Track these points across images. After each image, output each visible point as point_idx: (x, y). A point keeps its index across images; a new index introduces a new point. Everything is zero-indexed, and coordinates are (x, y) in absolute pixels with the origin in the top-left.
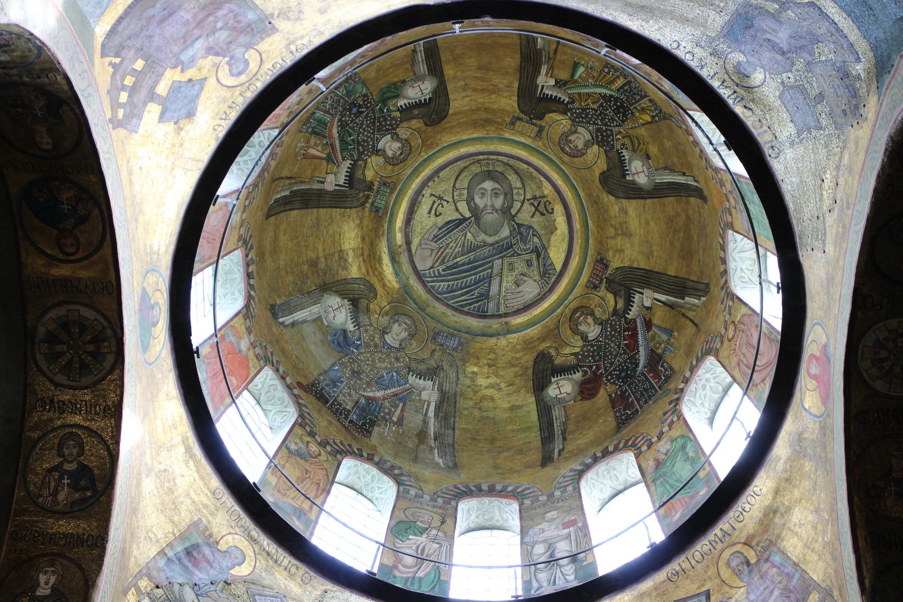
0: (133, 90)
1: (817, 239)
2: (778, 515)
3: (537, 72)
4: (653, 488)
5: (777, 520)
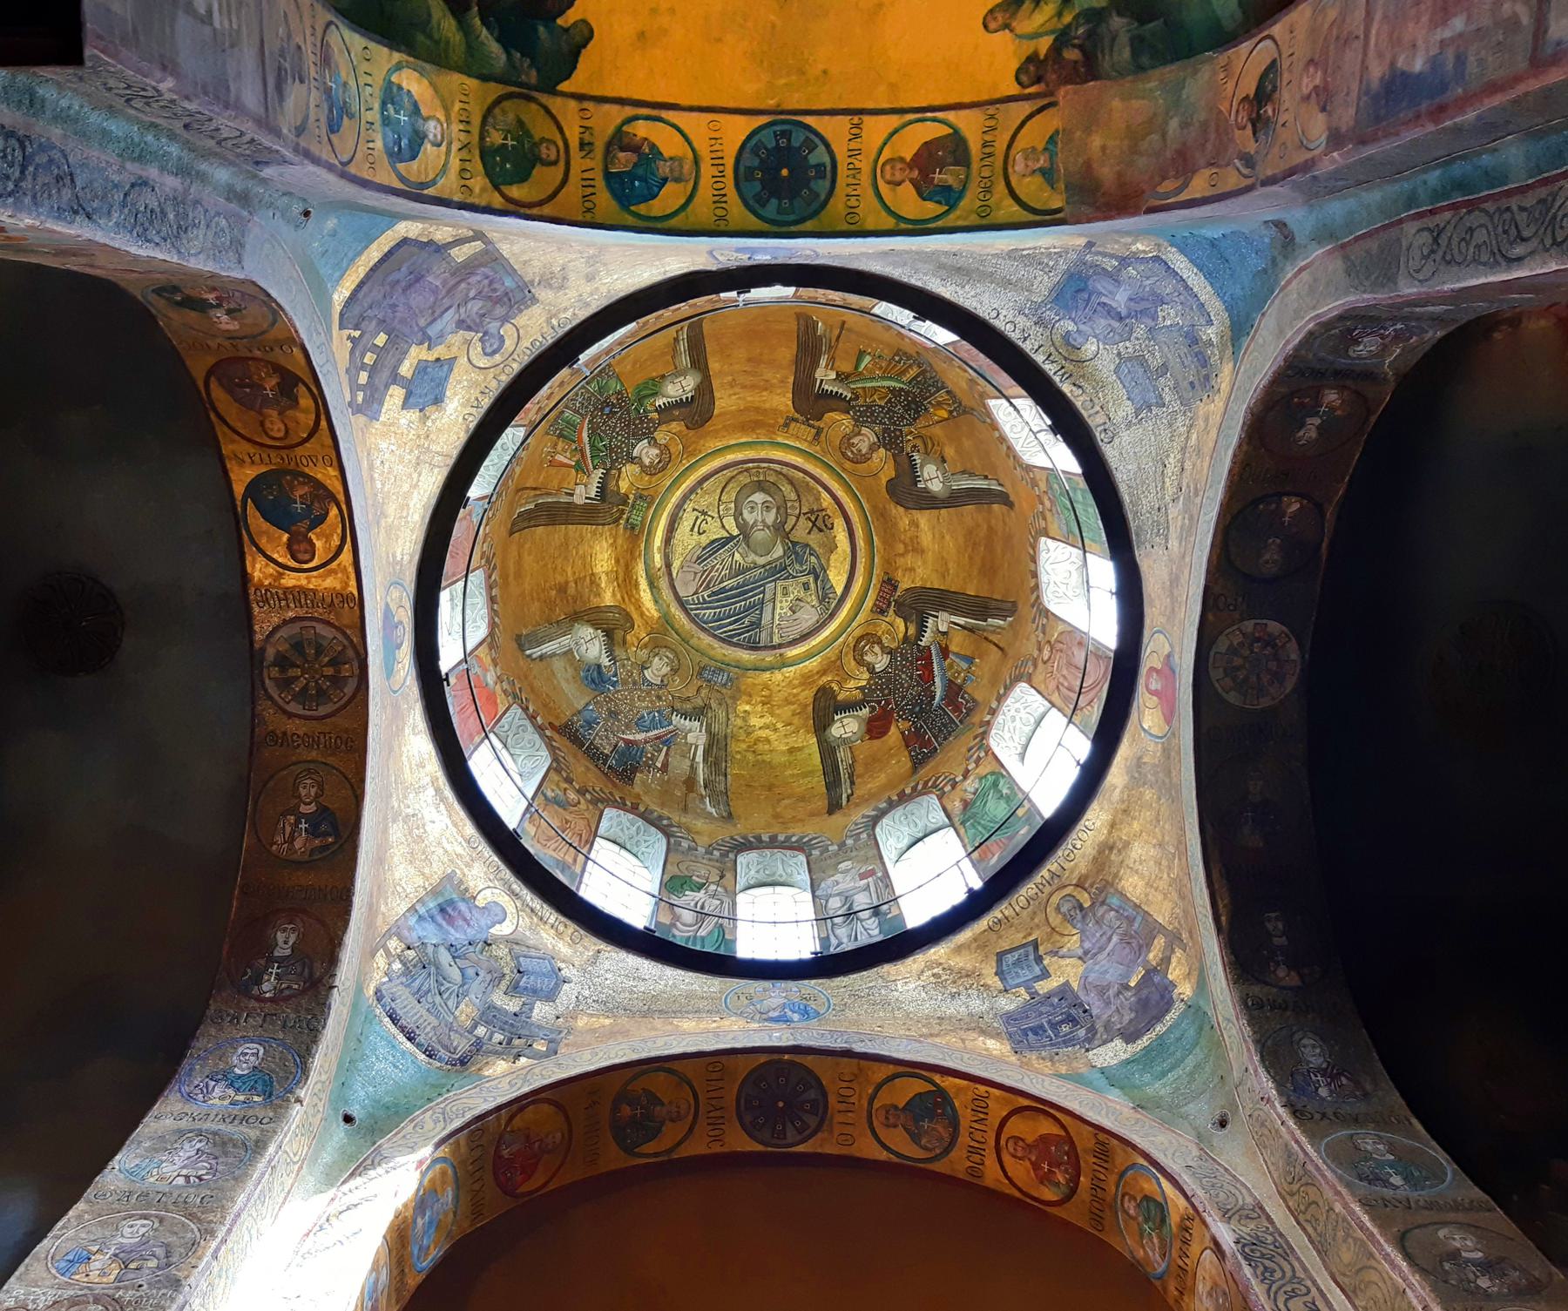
0: (373, 370)
1: (1158, 534)
2: (1115, 851)
3: (815, 364)
4: (962, 831)
5: (1113, 857)
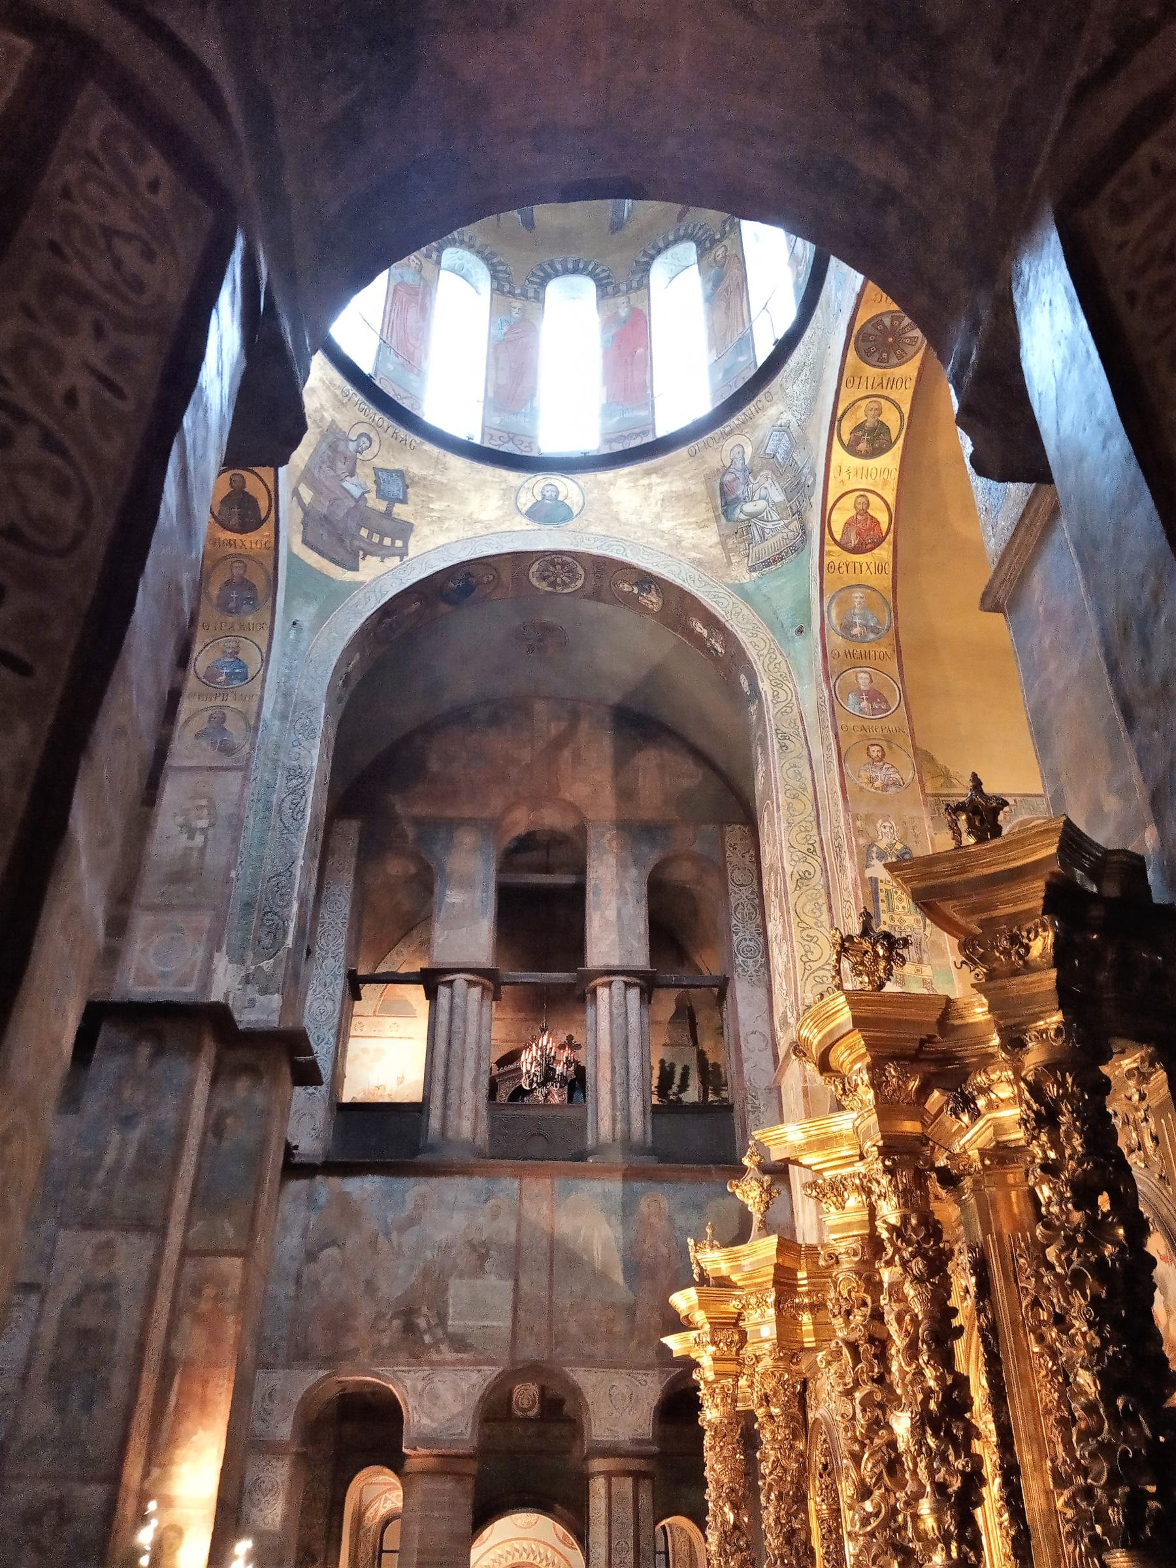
0: (383, 535)
